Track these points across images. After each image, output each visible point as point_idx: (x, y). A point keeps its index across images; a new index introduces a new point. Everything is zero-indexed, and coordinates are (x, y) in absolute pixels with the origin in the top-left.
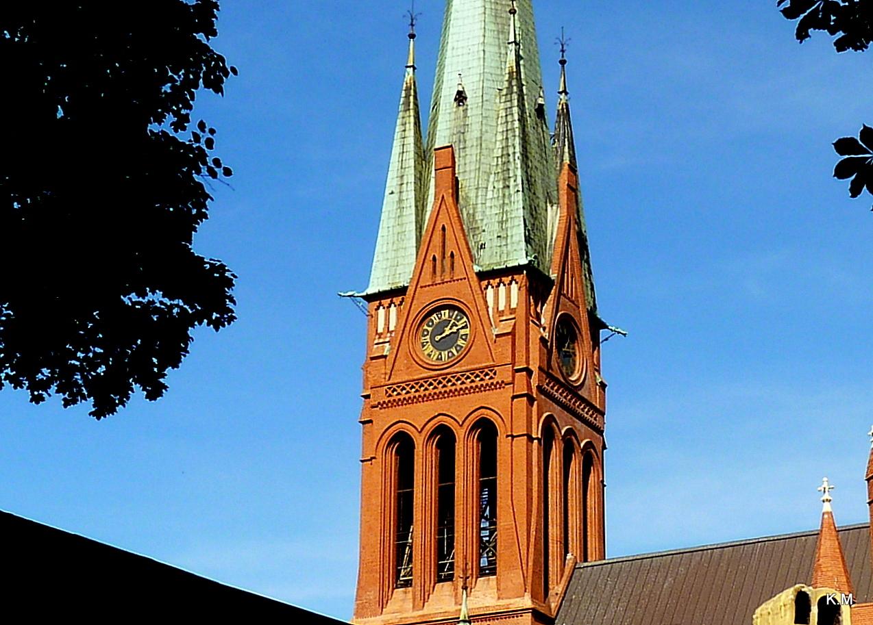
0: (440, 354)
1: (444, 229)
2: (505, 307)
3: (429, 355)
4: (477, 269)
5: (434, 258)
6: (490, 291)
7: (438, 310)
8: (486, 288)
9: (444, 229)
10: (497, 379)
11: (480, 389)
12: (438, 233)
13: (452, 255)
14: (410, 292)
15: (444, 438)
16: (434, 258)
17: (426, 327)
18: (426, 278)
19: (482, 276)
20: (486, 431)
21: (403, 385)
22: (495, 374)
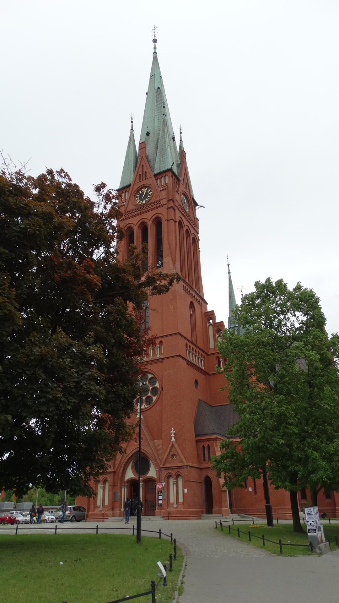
0: (143, 202)
1: (143, 165)
2: (164, 183)
3: (139, 203)
4: (154, 173)
5: (140, 174)
6: (159, 181)
7: (141, 189)
8: (157, 179)
9: (143, 165)
10: (162, 203)
11: (157, 208)
12: (141, 167)
13: (146, 172)
14: (132, 186)
15: (144, 228)
16: (140, 174)
17: (137, 195)
18: (138, 180)
19: (155, 175)
20: (158, 223)
21: (130, 212)
22: (161, 202)
